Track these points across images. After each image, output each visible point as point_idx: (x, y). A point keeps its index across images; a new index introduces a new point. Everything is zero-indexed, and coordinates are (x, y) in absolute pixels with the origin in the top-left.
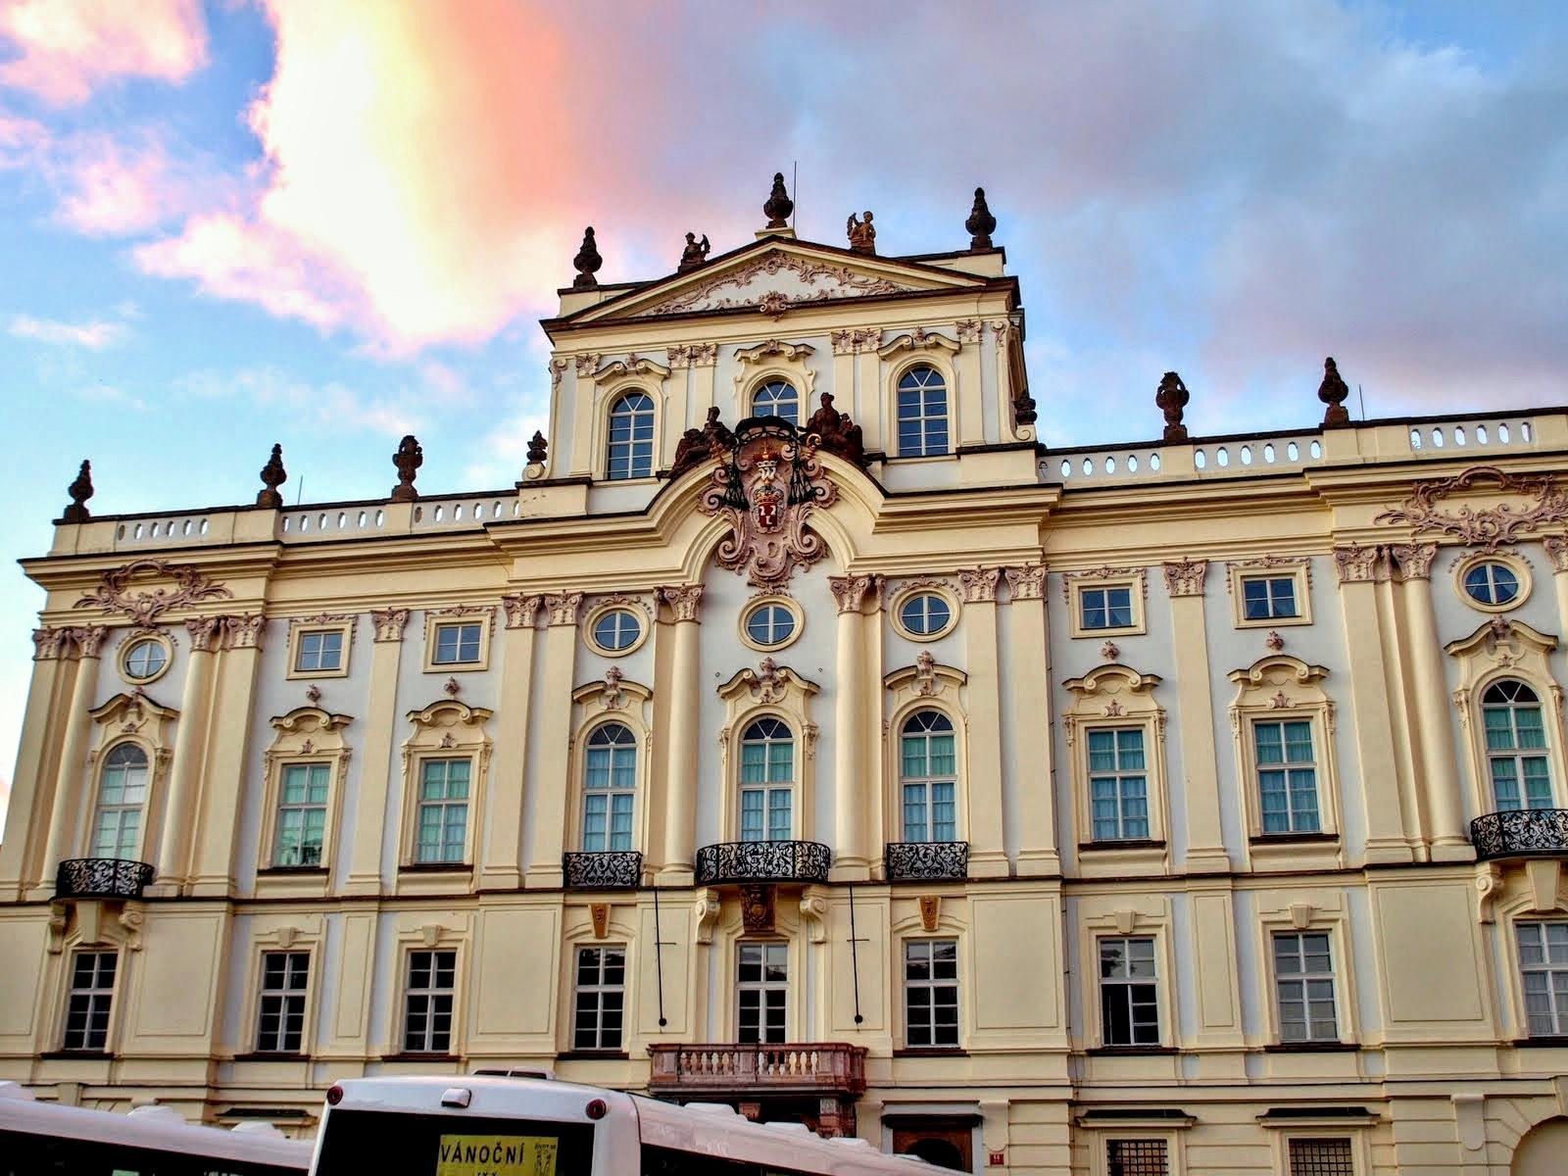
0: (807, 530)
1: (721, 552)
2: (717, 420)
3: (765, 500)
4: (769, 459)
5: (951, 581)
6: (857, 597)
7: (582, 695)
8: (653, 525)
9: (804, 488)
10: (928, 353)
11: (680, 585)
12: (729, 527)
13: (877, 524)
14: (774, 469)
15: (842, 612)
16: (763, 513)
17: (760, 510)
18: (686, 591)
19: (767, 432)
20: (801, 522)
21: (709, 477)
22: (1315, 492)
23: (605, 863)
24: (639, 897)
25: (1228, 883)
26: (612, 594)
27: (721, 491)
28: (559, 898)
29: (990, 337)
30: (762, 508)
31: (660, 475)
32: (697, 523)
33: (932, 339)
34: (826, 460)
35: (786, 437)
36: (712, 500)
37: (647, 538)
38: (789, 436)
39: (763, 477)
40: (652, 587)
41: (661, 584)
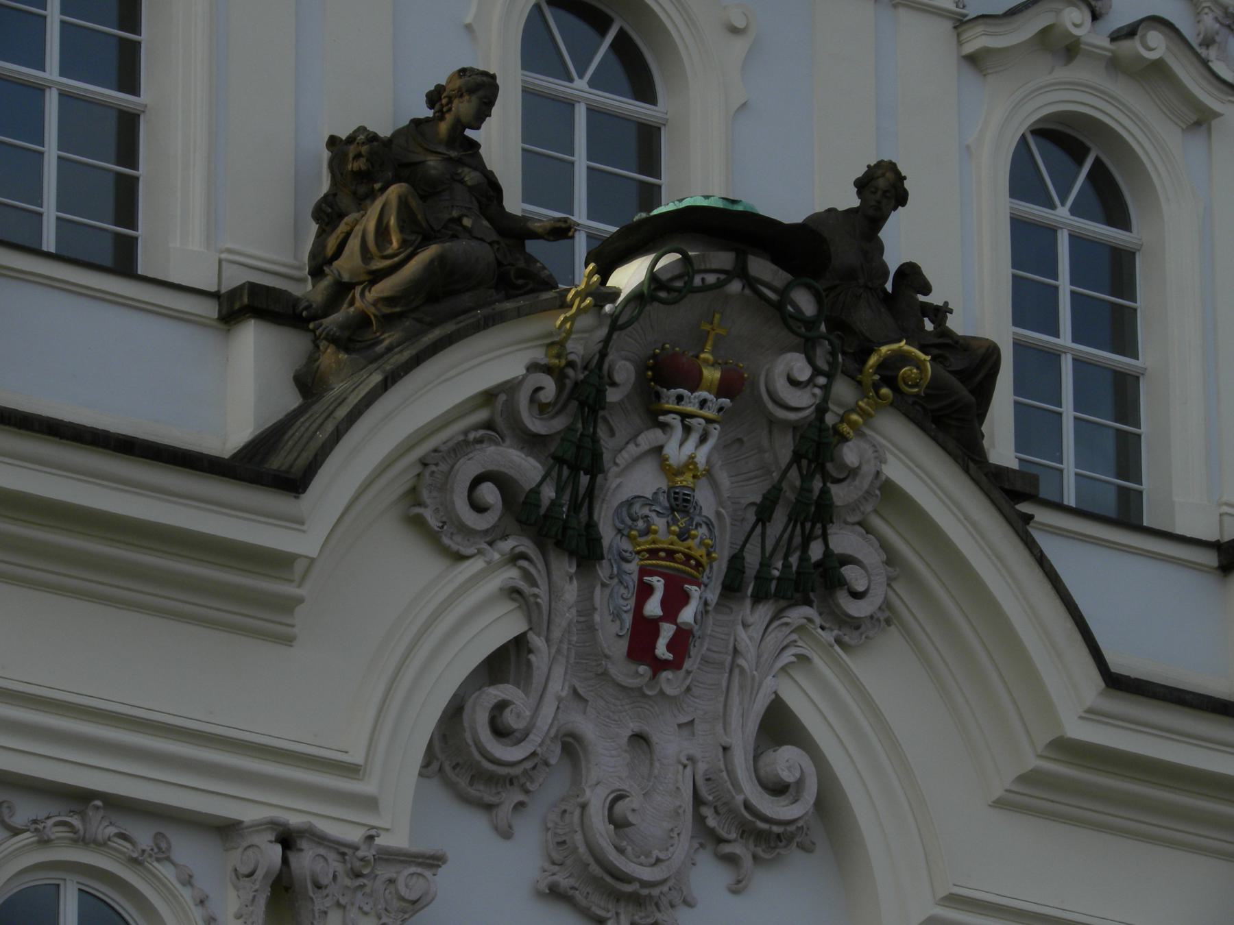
1: (478, 718)
2: (430, 113)
3: (671, 554)
4: (723, 389)
9: (805, 547)
10: (1119, 88)
11: (354, 835)
12: (503, 626)
14: (715, 431)
16: (653, 607)
17: (645, 591)
18: (363, 864)
19: (751, 283)
20: (769, 685)
26: (80, 798)
27: (527, 468)
30: (658, 583)
31: (246, 304)
32: (405, 574)
33: (1156, 45)
34: (903, 457)
35: (799, 317)
36: (489, 493)
38: (811, 324)
40: (248, 814)
41: (295, 812)
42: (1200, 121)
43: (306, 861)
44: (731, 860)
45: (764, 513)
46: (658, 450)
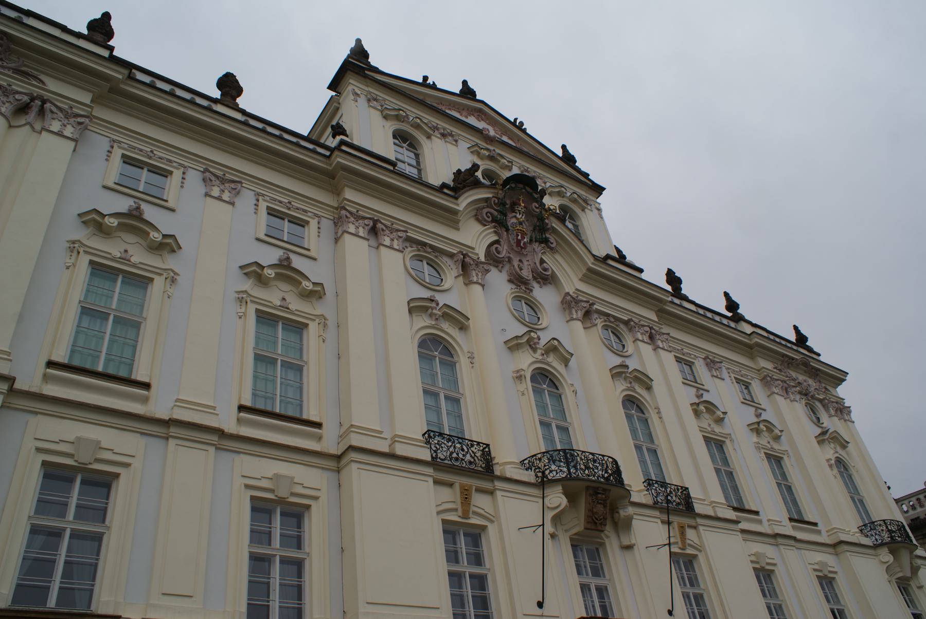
0: (542, 261)
5: (622, 326)
6: (580, 314)
7: (416, 308)
8: (461, 208)
12: (496, 238)
13: (584, 275)
15: (572, 319)
21: (486, 200)
22: (750, 347)
23: (465, 448)
24: (498, 484)
25: (792, 542)
26: (424, 244)
28: (429, 470)
29: (596, 211)
37: (451, 218)
39: (519, 216)
42: (583, 210)
43: (467, 259)
44: (539, 282)
45: (534, 230)
46: (515, 217)
